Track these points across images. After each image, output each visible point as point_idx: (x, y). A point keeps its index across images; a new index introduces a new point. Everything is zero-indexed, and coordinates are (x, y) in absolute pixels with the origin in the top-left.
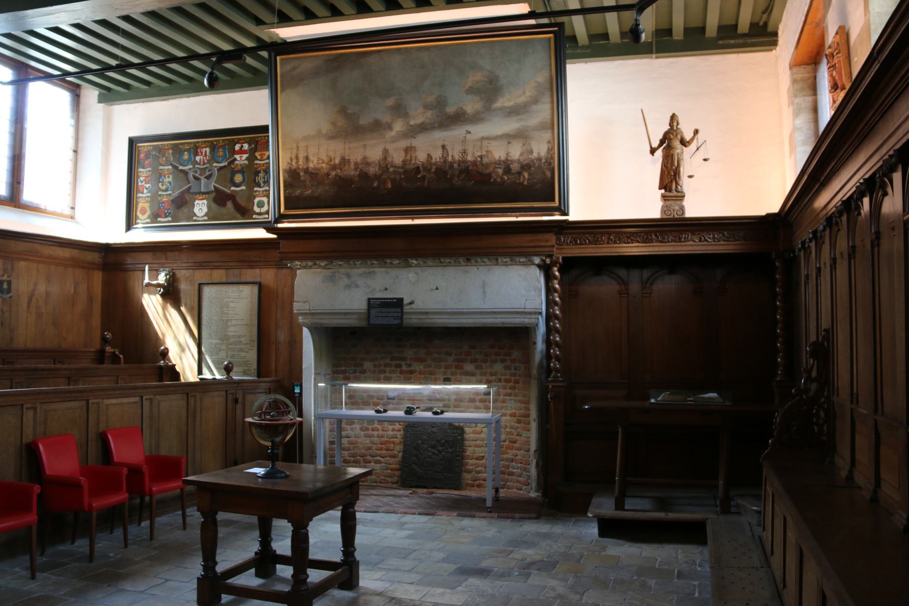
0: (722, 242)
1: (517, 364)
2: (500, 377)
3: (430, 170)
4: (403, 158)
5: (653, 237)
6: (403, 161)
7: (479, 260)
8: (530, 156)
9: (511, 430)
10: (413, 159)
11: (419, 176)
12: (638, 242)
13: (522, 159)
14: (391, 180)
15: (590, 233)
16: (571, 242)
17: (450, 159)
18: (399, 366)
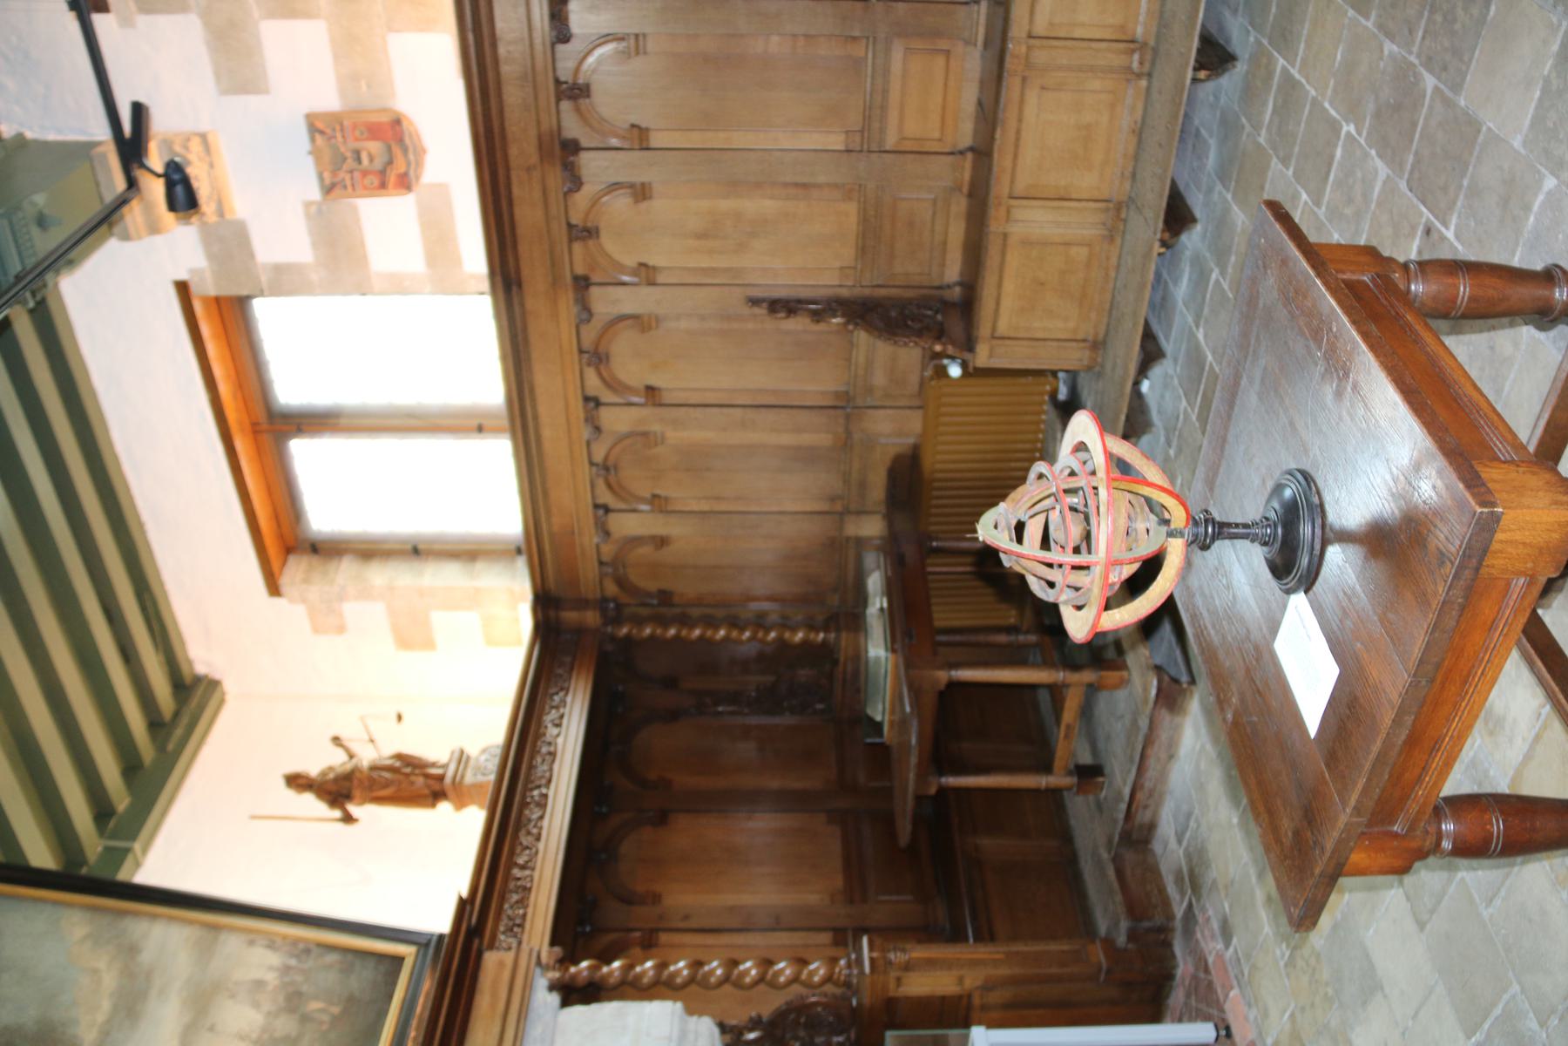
5: (536, 793)
8: (270, 988)
12: (541, 817)
13: (267, 1006)
15: (502, 899)
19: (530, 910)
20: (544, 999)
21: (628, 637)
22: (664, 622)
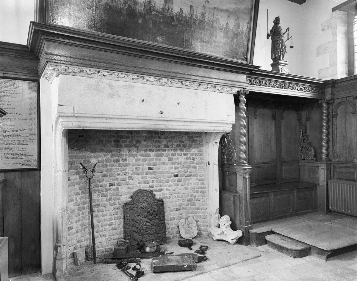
0: (307, 92)
1: (194, 156)
2: (183, 165)
3: (181, 21)
4: (163, 7)
6: (163, 8)
10: (170, 9)
11: (173, 24)
14: (153, 21)
17: (194, 17)
18: (117, 161)
20: (235, 91)
21: (323, 106)
22: (327, 116)
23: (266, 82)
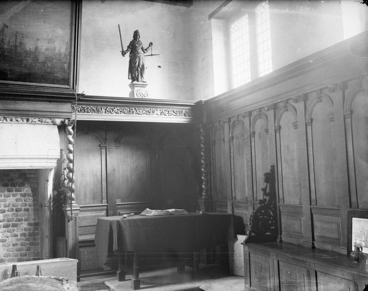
1: (27, 197)
7: (19, 119)
9: (22, 247)
16: (81, 110)
19: (91, 113)
23: (107, 108)
